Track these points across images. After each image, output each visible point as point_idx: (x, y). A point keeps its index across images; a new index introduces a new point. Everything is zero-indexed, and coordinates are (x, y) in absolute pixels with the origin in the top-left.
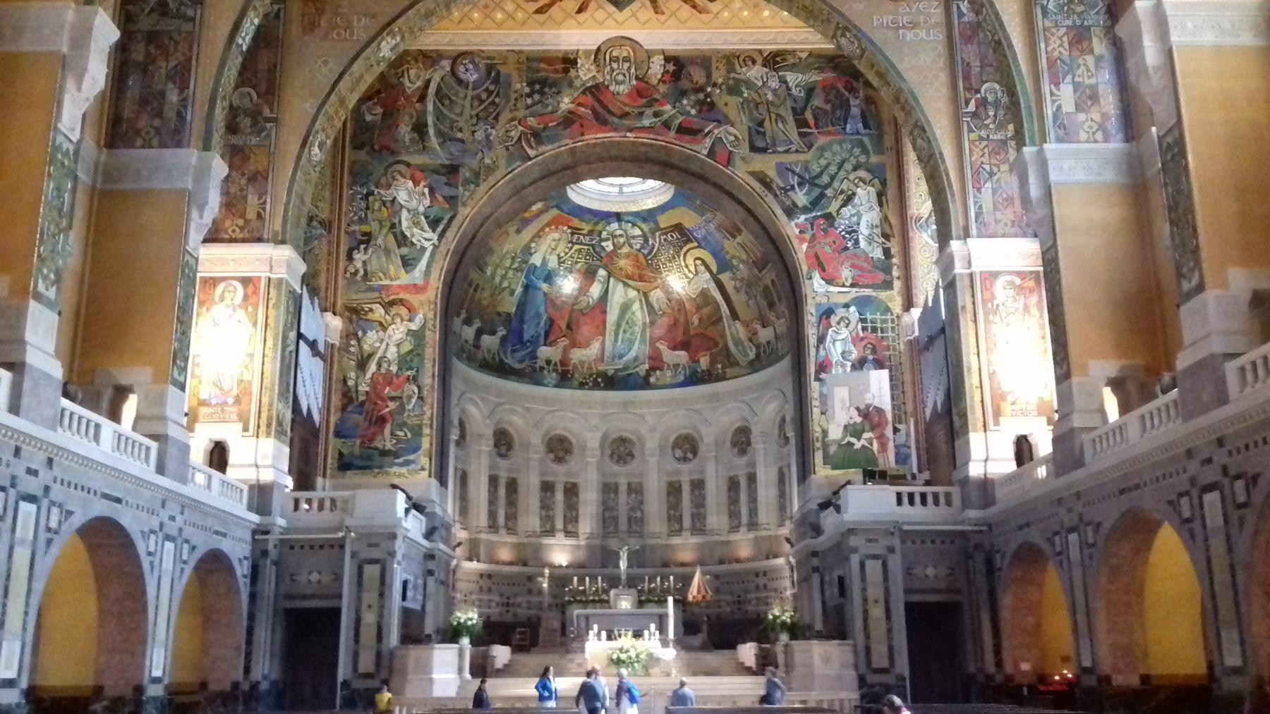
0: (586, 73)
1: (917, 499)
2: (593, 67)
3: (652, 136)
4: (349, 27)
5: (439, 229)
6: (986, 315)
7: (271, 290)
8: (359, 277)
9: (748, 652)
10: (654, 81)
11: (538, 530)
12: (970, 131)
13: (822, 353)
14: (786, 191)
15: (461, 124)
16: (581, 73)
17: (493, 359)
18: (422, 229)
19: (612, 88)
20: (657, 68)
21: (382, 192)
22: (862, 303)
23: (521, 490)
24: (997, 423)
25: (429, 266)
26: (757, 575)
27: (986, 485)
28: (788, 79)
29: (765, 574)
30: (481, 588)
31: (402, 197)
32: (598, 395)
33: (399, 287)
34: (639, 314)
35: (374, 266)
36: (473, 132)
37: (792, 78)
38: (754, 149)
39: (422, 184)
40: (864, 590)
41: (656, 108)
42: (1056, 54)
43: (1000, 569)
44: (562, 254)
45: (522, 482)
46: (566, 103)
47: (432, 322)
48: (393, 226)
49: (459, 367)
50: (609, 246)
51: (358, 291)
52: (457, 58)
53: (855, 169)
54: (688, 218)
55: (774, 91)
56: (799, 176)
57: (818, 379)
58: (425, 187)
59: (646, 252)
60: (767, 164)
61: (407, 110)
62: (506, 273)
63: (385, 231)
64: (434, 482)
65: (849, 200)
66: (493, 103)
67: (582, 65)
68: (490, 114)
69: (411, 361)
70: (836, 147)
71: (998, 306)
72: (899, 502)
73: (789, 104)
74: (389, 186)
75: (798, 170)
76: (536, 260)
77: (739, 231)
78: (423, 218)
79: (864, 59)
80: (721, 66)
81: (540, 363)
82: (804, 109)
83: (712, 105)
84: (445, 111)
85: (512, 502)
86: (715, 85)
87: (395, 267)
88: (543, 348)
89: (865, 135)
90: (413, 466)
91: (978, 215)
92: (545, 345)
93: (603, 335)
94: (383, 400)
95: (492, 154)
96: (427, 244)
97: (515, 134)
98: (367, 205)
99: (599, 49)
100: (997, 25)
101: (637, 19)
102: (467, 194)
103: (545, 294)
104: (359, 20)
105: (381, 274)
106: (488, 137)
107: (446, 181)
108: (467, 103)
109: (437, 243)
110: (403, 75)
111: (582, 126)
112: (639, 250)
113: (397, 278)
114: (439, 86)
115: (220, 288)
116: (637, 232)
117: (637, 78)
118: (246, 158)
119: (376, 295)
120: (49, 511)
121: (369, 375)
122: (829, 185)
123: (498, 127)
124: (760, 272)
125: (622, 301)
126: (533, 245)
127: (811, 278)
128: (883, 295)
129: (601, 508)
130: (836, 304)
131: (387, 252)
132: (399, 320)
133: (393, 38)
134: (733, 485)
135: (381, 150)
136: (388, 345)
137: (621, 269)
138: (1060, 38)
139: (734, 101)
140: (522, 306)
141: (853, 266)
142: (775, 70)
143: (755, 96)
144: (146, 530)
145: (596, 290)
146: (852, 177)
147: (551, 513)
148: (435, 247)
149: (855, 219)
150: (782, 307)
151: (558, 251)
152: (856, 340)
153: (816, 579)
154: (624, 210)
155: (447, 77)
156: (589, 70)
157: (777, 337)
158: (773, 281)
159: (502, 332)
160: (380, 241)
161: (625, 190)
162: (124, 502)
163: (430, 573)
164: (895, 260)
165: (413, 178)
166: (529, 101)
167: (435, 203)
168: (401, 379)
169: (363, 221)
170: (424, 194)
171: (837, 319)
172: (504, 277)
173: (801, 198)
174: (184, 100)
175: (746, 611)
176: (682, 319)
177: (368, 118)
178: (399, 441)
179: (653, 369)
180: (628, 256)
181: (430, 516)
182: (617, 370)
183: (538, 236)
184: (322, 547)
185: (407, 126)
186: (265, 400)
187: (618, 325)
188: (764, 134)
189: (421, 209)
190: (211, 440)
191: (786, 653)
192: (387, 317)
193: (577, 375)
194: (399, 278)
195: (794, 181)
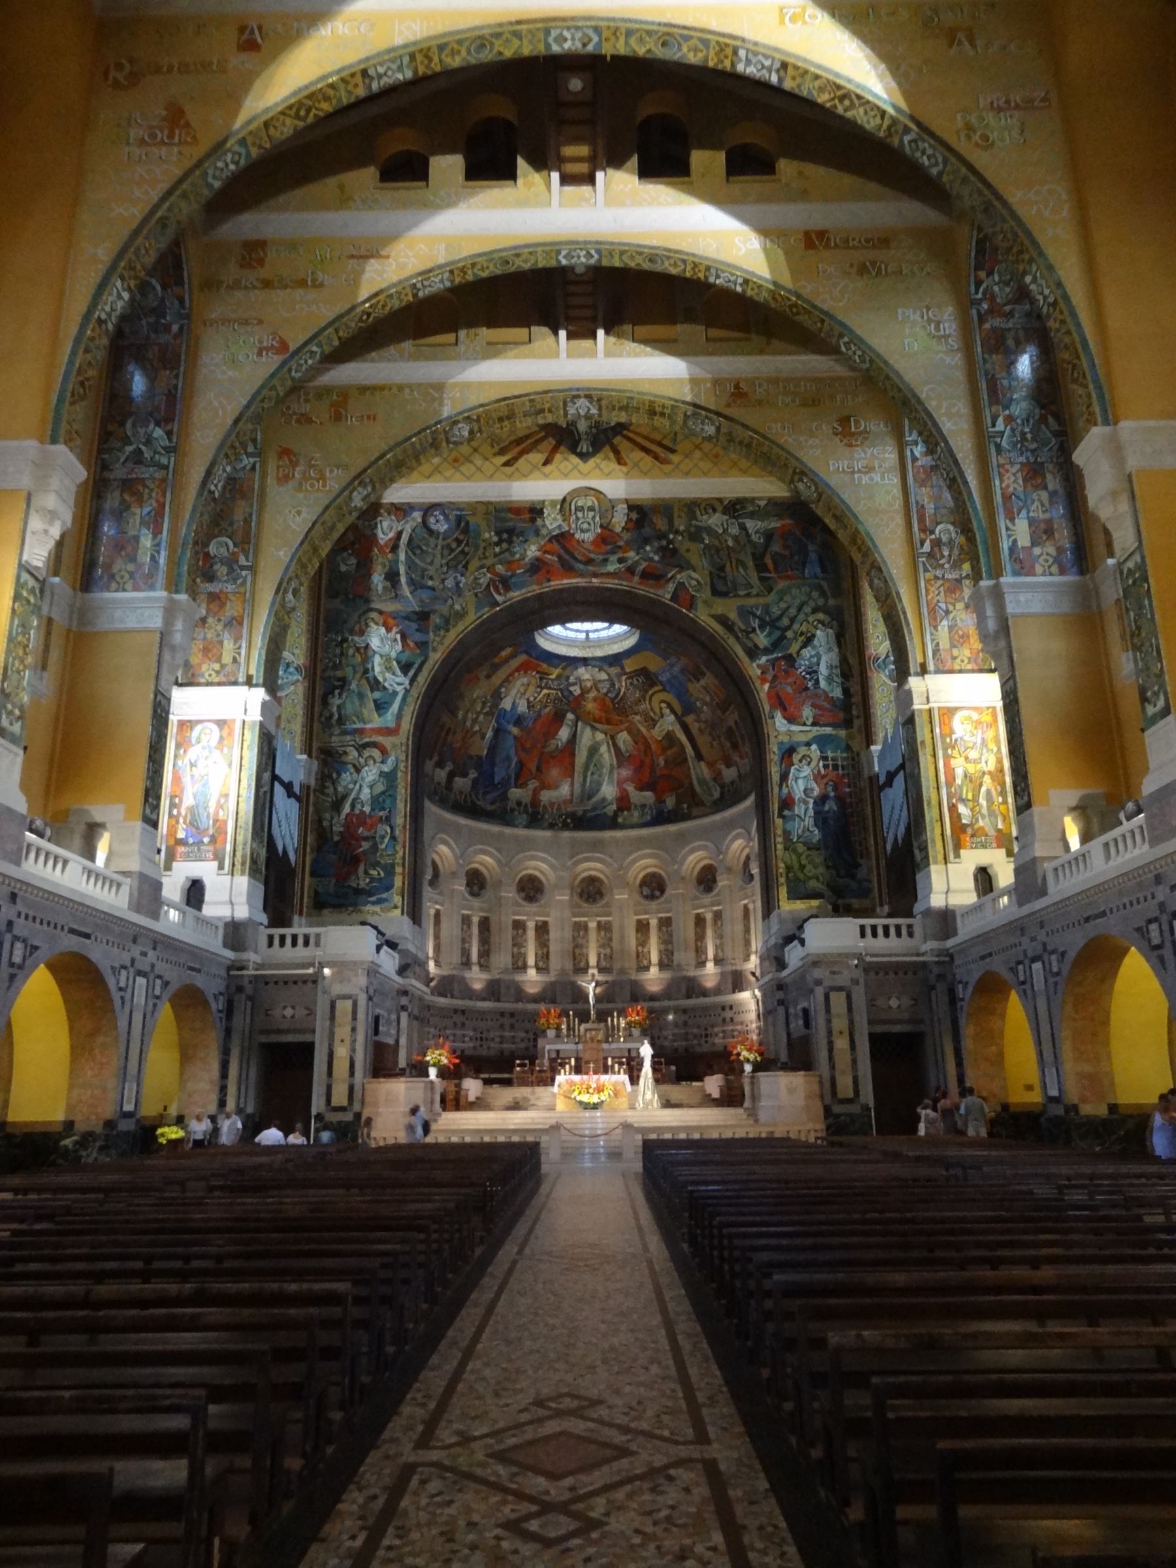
0: (552, 522)
1: (880, 931)
2: (559, 517)
3: (616, 581)
4: (322, 477)
6: (945, 750)
7: (246, 732)
9: (713, 1084)
10: (618, 529)
11: (510, 966)
12: (926, 570)
13: (785, 791)
14: (748, 633)
15: (431, 571)
16: (547, 522)
17: (465, 801)
18: (394, 674)
19: (577, 536)
22: (822, 741)
23: (494, 927)
24: (957, 856)
25: (401, 709)
26: (723, 1008)
27: (946, 919)
28: (748, 526)
29: (731, 1007)
30: (455, 1024)
32: (566, 834)
33: (372, 729)
34: (606, 756)
35: (349, 709)
36: (443, 581)
37: (751, 525)
38: (716, 592)
39: (395, 630)
40: (829, 1021)
41: (620, 555)
42: (1011, 489)
43: (963, 1000)
44: (532, 699)
45: (494, 919)
48: (366, 671)
49: (432, 809)
50: (576, 690)
52: (428, 509)
53: (815, 611)
54: (653, 662)
55: (735, 538)
56: (761, 619)
57: (781, 816)
59: (612, 695)
60: (729, 608)
61: (380, 560)
62: (477, 718)
63: (358, 676)
64: (406, 920)
65: (809, 641)
66: (462, 552)
67: (549, 515)
68: (459, 562)
69: (384, 801)
70: (794, 591)
71: (956, 740)
72: (863, 935)
73: (749, 550)
74: (362, 633)
75: (758, 613)
76: (506, 704)
77: (703, 674)
78: (395, 663)
79: (821, 504)
80: (683, 515)
81: (511, 804)
82: (763, 555)
83: (675, 551)
84: (417, 561)
86: (677, 532)
87: (369, 710)
88: (514, 790)
89: (823, 579)
90: (386, 904)
91: (936, 651)
92: (516, 787)
93: (572, 776)
95: (461, 600)
96: (399, 689)
97: (483, 581)
99: (564, 500)
100: (951, 462)
101: (601, 470)
102: (437, 639)
103: (515, 737)
104: (332, 471)
106: (457, 584)
108: (438, 551)
110: (376, 527)
111: (548, 572)
112: (606, 694)
113: (370, 721)
114: (410, 540)
115: (197, 729)
116: (604, 676)
117: (601, 526)
118: (222, 605)
120: (12, 946)
121: (343, 816)
122: (789, 628)
123: (468, 574)
124: (724, 713)
125: (590, 743)
126: (503, 690)
127: (773, 717)
128: (842, 733)
129: (572, 945)
130: (799, 744)
132: (371, 762)
133: (365, 486)
136: (361, 786)
137: (589, 713)
138: (1014, 475)
139: (696, 547)
140: (493, 748)
141: (814, 706)
142: (734, 517)
143: (716, 543)
144: (116, 965)
145: (564, 734)
146: (811, 619)
147: (523, 950)
148: (407, 691)
149: (815, 660)
150: (746, 748)
151: (527, 696)
152: (817, 777)
153: (781, 1010)
154: (590, 655)
156: (555, 519)
157: (740, 776)
158: (736, 723)
159: (473, 774)
160: (353, 686)
161: (592, 635)
162: (93, 937)
163: (404, 1008)
164: (853, 700)
165: (385, 625)
166: (497, 549)
170: (395, 640)
171: (799, 757)
172: (475, 721)
173: (762, 639)
175: (714, 1044)
176: (648, 761)
177: (343, 568)
178: (372, 880)
179: (620, 809)
180: (595, 700)
181: (404, 953)
182: (585, 811)
183: (507, 680)
184: (295, 983)
186: (240, 839)
187: (586, 767)
188: (725, 578)
189: (393, 654)
190: (187, 878)
191: (752, 1083)
193: (547, 816)
195: (756, 624)
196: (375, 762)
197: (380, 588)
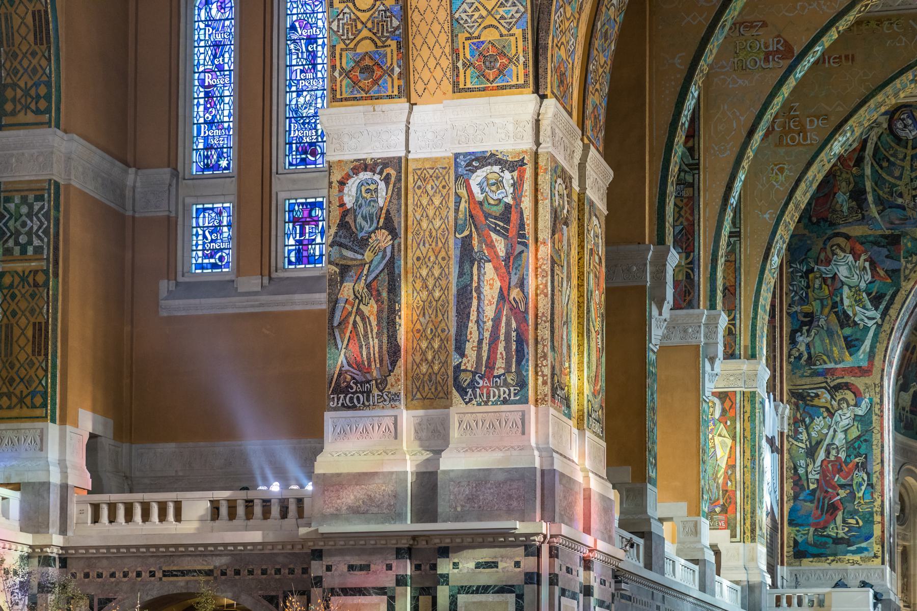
5: (882, 307)
7: (746, 403)
8: (802, 361)
18: (864, 307)
21: (822, 268)
25: (873, 347)
31: (843, 272)
33: (844, 369)
35: (817, 348)
39: (863, 257)
47: (879, 406)
48: (835, 305)
51: (802, 376)
58: (865, 260)
63: (827, 310)
69: (859, 447)
74: (828, 262)
78: (864, 295)
94: (834, 488)
96: (870, 323)
98: (808, 283)
102: (910, 266)
105: (825, 357)
107: (887, 253)
109: (880, 322)
119: (821, 379)
121: (818, 463)
131: (830, 333)
132: (845, 405)
135: (818, 222)
136: (835, 431)
148: (879, 326)
155: (883, 138)
160: (822, 322)
165: (852, 252)
167: (876, 278)
168: (850, 466)
169: (804, 301)
170: (865, 268)
174: (691, 263)
185: (845, 194)
189: (863, 285)
192: (833, 402)
194: (843, 361)
196: (848, 405)
197: (845, 209)
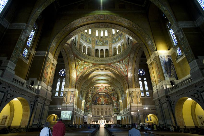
0: (100, 87)
20: (104, 87)
22: (116, 102)
31: (89, 95)
46: (99, 89)
85: (95, 113)
87: (89, 99)
134: (109, 112)
140: (96, 100)
173: (112, 95)
